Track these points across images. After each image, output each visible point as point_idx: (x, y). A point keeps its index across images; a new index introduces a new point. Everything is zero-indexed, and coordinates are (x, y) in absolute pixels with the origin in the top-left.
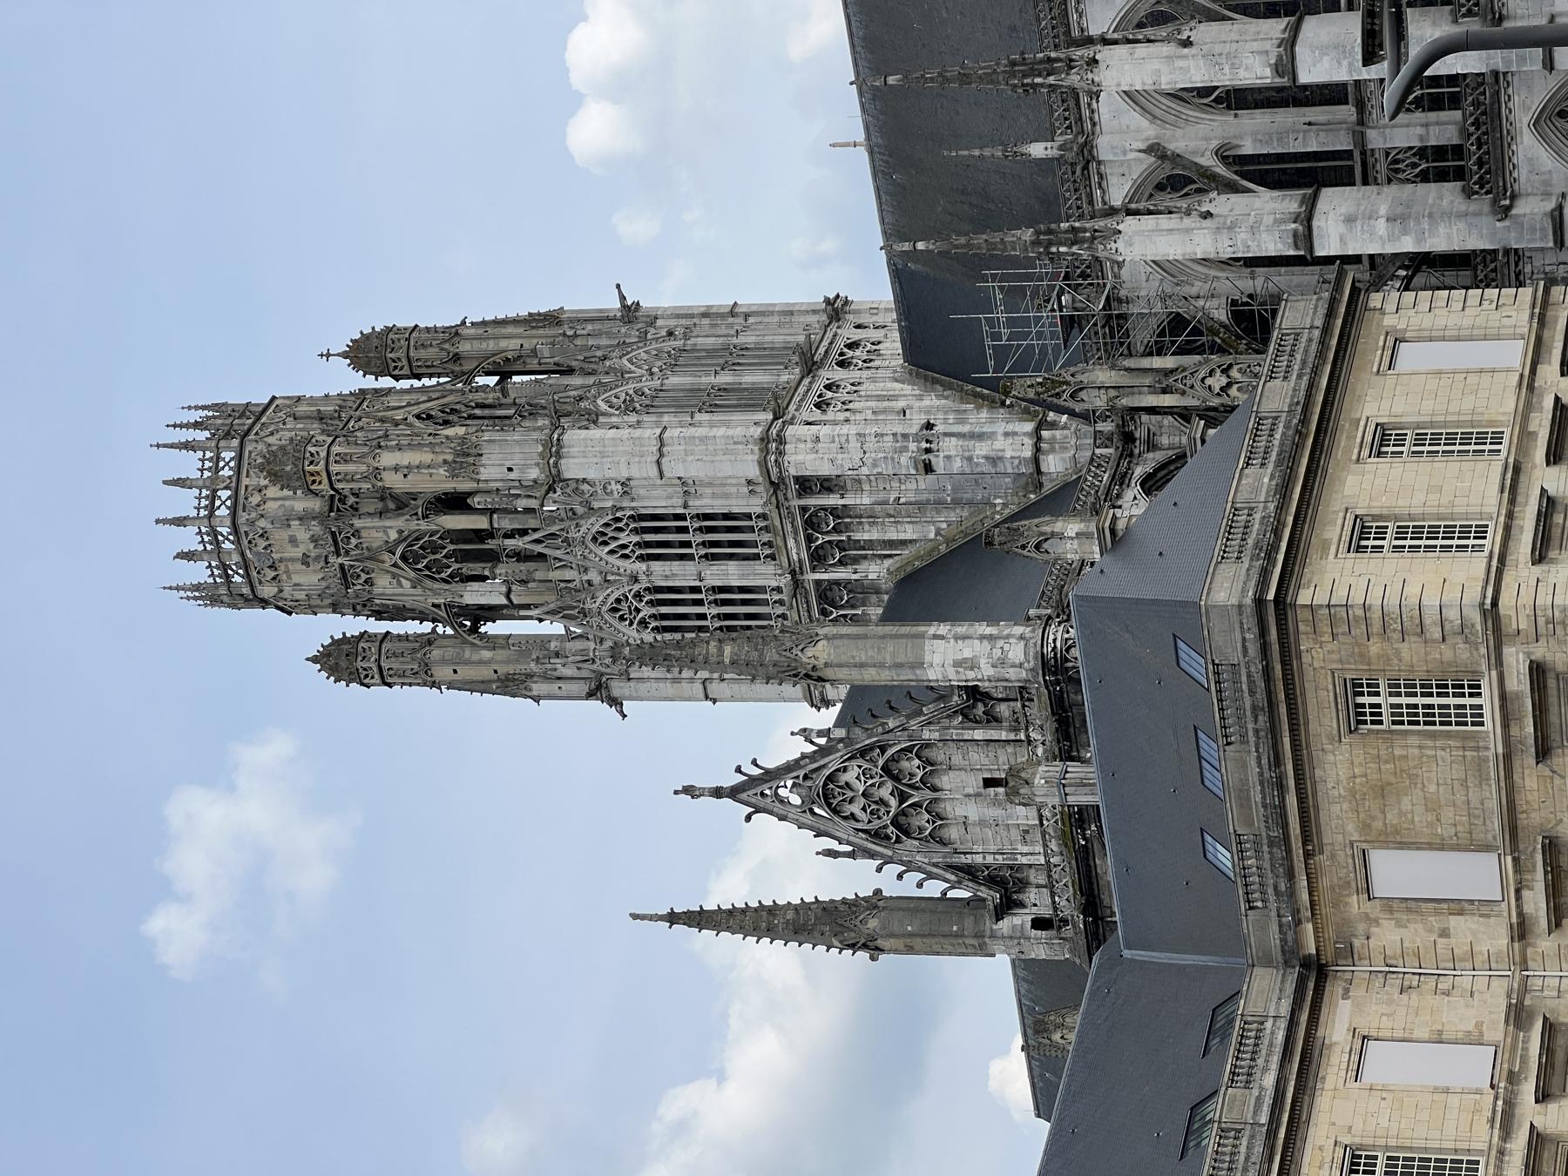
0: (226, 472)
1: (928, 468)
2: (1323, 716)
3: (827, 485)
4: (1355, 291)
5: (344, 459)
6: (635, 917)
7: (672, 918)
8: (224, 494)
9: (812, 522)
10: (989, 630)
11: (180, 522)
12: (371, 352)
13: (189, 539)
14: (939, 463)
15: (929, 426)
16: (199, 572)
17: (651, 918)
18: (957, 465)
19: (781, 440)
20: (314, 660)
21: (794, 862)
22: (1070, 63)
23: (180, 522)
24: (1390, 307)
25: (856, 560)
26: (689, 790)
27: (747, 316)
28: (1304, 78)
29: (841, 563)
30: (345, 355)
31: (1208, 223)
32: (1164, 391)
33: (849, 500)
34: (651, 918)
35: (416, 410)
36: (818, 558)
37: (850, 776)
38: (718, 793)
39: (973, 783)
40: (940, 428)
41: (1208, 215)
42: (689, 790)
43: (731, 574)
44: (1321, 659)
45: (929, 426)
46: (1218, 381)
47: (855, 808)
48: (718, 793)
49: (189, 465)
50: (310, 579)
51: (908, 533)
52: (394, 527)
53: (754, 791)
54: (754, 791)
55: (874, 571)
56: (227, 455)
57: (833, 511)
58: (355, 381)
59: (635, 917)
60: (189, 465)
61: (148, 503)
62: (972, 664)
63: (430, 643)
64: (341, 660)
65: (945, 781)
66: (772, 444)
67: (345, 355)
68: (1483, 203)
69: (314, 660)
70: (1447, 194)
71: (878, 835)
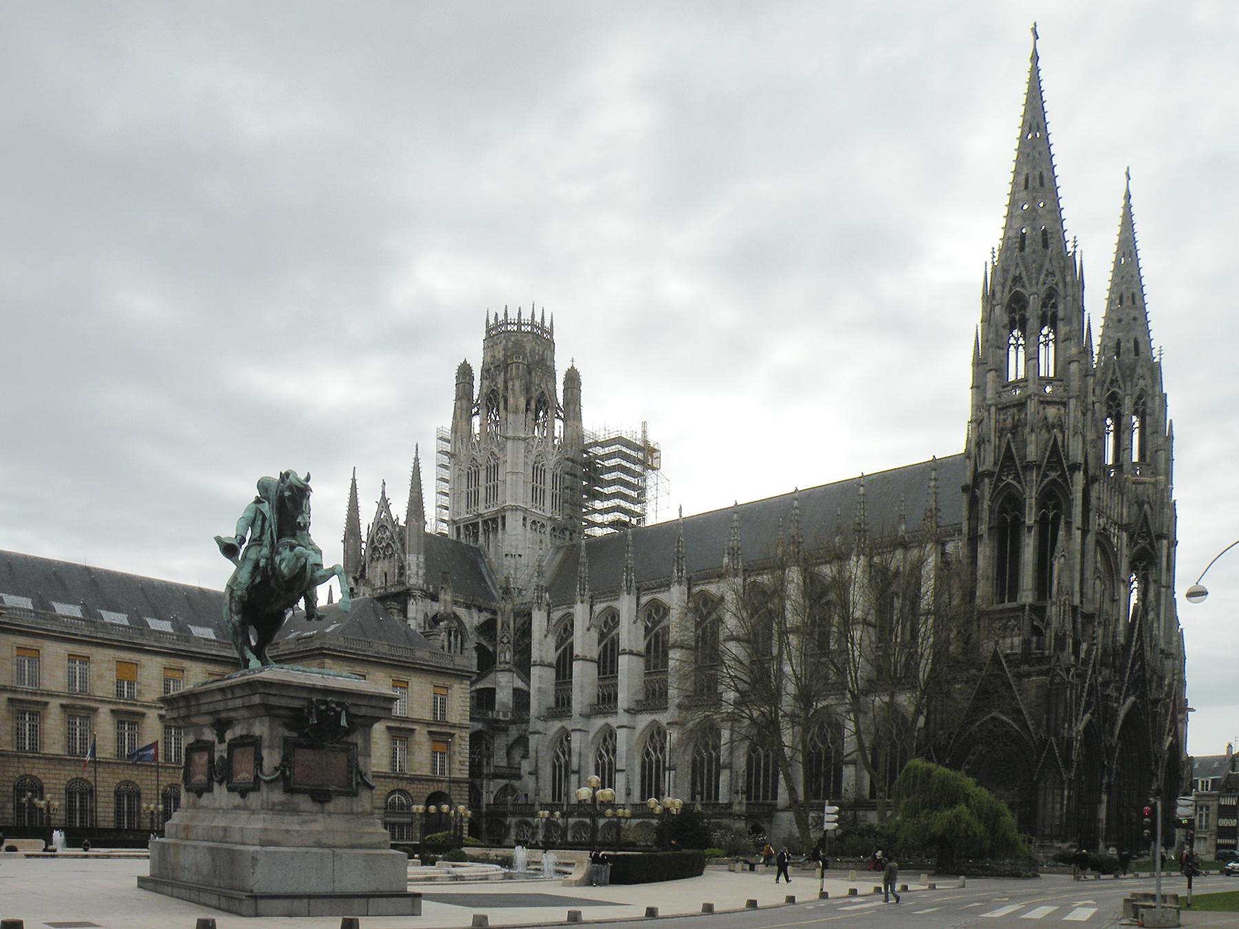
5: (518, 368)
46: (505, 640)
49: (526, 316)
56: (529, 329)
60: (526, 316)
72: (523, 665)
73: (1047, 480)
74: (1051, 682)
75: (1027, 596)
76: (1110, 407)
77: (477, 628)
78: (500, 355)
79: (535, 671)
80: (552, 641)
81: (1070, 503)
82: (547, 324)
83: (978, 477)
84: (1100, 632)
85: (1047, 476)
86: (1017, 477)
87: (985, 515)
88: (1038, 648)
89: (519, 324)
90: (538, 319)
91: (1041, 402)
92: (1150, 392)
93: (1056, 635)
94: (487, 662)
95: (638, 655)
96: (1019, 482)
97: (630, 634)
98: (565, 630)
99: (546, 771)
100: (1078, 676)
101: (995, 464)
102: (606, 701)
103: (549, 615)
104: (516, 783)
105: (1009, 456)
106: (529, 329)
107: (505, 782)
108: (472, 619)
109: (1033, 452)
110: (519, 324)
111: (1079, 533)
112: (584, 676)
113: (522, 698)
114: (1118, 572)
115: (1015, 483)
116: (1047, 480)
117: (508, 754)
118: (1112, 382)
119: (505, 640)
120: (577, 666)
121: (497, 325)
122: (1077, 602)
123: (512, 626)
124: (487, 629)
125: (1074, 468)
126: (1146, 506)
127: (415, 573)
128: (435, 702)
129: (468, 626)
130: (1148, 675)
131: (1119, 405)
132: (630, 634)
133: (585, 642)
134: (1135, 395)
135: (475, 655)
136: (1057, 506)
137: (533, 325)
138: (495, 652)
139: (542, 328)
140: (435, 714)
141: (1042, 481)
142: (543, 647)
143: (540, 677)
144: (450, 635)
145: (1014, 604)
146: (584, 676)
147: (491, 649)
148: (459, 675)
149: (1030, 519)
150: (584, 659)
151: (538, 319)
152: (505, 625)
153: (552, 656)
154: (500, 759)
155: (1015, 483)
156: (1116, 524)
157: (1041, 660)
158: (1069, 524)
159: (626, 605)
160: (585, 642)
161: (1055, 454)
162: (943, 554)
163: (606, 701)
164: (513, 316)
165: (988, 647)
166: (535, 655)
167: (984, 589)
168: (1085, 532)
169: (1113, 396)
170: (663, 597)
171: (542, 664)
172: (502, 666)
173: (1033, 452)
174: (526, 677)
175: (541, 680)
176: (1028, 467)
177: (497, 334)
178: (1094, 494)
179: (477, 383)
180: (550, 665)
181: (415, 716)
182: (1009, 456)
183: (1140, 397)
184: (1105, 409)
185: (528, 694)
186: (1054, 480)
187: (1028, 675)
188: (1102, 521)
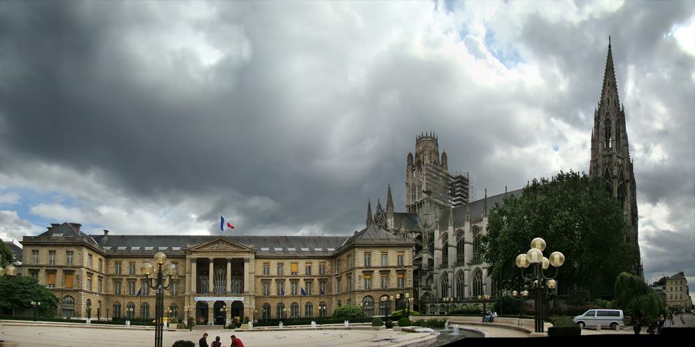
9: (421, 203)
13: (421, 136)
36: (418, 205)
44: (352, 252)
49: (429, 135)
55: (417, 210)
58: (441, 153)
60: (429, 135)
64: (410, 155)
68: (438, 266)
72: (432, 250)
79: (436, 252)
80: (441, 241)
90: (433, 136)
98: (446, 236)
99: (440, 287)
102: (460, 261)
104: (429, 291)
107: (425, 291)
112: (452, 252)
113: (431, 261)
117: (427, 282)
120: (449, 249)
124: (419, 238)
132: (469, 236)
133: (452, 240)
137: (431, 138)
142: (438, 243)
146: (452, 252)
151: (433, 136)
152: (425, 237)
153: (441, 246)
154: (424, 283)
159: (467, 227)
163: (460, 261)
164: (424, 135)
166: (436, 246)
171: (438, 249)
174: (433, 254)
175: (438, 254)
177: (419, 141)
179: (414, 160)
180: (440, 250)
185: (433, 260)
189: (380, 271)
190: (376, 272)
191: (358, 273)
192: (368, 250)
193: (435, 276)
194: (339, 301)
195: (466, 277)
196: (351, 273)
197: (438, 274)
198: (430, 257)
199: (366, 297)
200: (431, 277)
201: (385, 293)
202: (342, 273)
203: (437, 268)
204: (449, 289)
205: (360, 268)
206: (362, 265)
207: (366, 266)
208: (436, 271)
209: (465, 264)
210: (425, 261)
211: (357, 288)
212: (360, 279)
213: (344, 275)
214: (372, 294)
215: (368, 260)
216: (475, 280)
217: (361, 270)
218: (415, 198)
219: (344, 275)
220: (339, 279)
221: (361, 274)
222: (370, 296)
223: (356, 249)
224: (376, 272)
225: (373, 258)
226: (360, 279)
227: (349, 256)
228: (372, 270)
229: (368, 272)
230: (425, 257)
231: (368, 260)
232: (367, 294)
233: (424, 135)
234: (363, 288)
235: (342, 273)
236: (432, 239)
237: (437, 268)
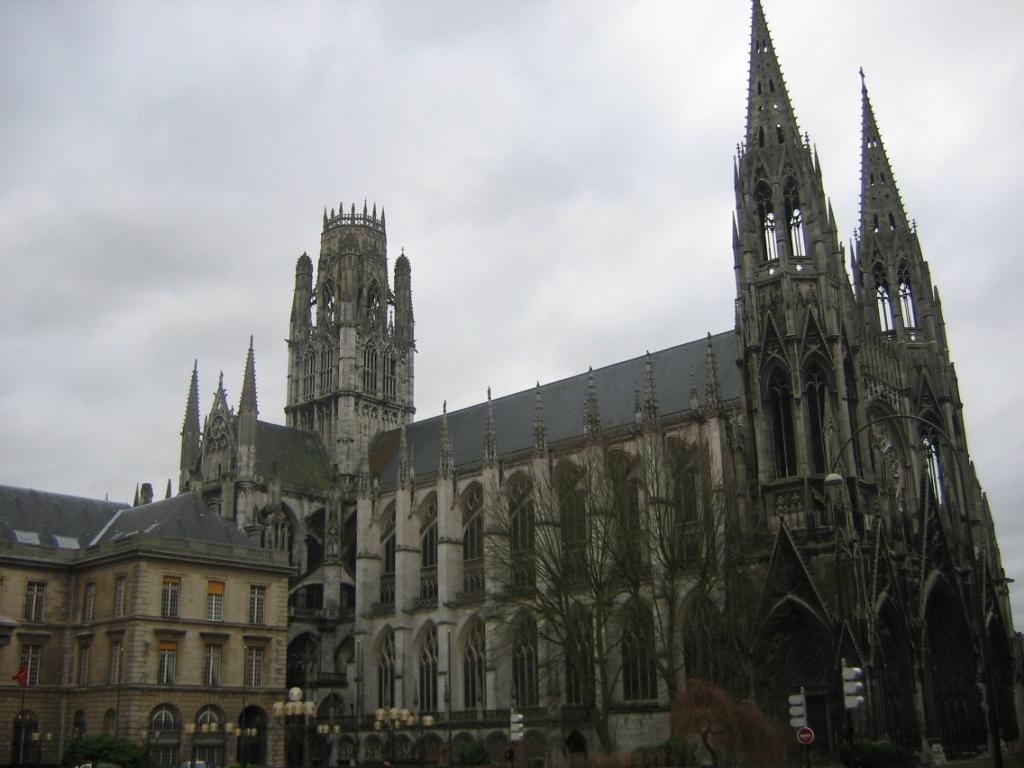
0: (356, 222)
1: (339, 441)
2: (118, 569)
3: (337, 410)
4: (288, 574)
5: (350, 258)
6: (196, 361)
7: (195, 372)
8: (349, 222)
10: (252, 464)
11: (341, 210)
12: (403, 265)
13: (337, 213)
14: (341, 444)
15: (352, 441)
16: (329, 217)
17: (196, 367)
18: (339, 450)
19: (349, 395)
20: (305, 254)
21: (205, 409)
22: (403, 482)
23: (341, 210)
24: (282, 584)
25: (319, 420)
26: (222, 375)
27: (409, 381)
28: (397, 555)
29: (319, 416)
30: (403, 255)
31: (367, 527)
32: (331, 516)
33: (333, 418)
34: (196, 367)
35: (377, 279)
37: (223, 425)
38: (221, 384)
39: (219, 461)
40: (351, 444)
41: (371, 526)
42: (222, 375)
43: (317, 380)
44: (129, 568)
45: (352, 441)
46: (333, 532)
47: (216, 427)
48: (221, 384)
49: (359, 211)
50: (325, 252)
51: (325, 435)
52: (335, 275)
53: (221, 395)
54: (221, 395)
55: (316, 426)
56: (362, 222)
57: (331, 413)
59: (196, 361)
60: (359, 211)
61: (353, 199)
62: (241, 460)
63: (307, 290)
64: (304, 263)
65: (221, 453)
66: (347, 394)
67: (403, 255)
69: (305, 254)
70: (376, 596)
71: (209, 433)
73: (808, 353)
74: (838, 558)
75: (805, 470)
76: (877, 277)
77: (307, 519)
78: (335, 247)
79: (360, 564)
81: (833, 373)
82: (379, 217)
83: (748, 352)
84: (885, 505)
85: (809, 349)
86: (781, 352)
87: (758, 389)
88: (823, 523)
89: (353, 218)
90: (370, 213)
91: (759, 288)
92: (910, 261)
93: (835, 509)
94: (316, 558)
95: (456, 543)
96: (784, 356)
97: (449, 523)
98: (389, 518)
100: (865, 551)
101: (760, 340)
103: (412, 494)
105: (771, 331)
106: (362, 222)
108: (302, 509)
109: (792, 327)
110: (353, 218)
111: (845, 405)
112: (406, 566)
114: (907, 439)
115: (779, 357)
116: (808, 353)
118: (875, 253)
119: (333, 532)
120: (399, 557)
121: (334, 219)
122: (853, 473)
123: (339, 516)
124: (316, 520)
125: (832, 340)
126: (924, 371)
127: (247, 470)
128: (252, 603)
129: (298, 517)
130: (950, 544)
131: (884, 275)
133: (407, 532)
134: (898, 264)
135: (305, 548)
136: (822, 378)
137: (365, 218)
138: (323, 544)
139: (374, 220)
140: (252, 617)
141: (804, 354)
142: (368, 539)
143: (365, 570)
144: (277, 528)
145: (794, 478)
146: (406, 566)
147: (320, 541)
148: (276, 573)
149: (798, 392)
150: (406, 550)
151: (370, 213)
155: (779, 357)
156: (895, 389)
157: (827, 536)
158: (834, 395)
160: (407, 532)
161: (813, 329)
162: (728, 428)
164: (347, 211)
165: (774, 521)
166: (360, 547)
167: (764, 464)
168: (853, 402)
169: (878, 267)
170: (480, 479)
171: (367, 557)
172: (330, 561)
173: (792, 327)
175: (366, 573)
176: (789, 341)
177: (333, 226)
178: (857, 365)
179: (315, 274)
181: (231, 619)
182: (771, 331)
183: (902, 267)
184: (872, 279)
186: (815, 353)
187: (816, 552)
188: (880, 388)
189: (203, 635)
190: (192, 635)
191: (143, 634)
192: (174, 571)
193: (358, 639)
194: (80, 713)
195: (443, 647)
196: (122, 632)
197: (367, 632)
198: (346, 579)
199: (159, 707)
200: (348, 642)
201: (214, 700)
202: (95, 625)
203: (364, 616)
204: (398, 684)
205: (148, 620)
206: (154, 611)
207: (164, 614)
208: (361, 624)
209: (440, 604)
210: (331, 593)
211: (136, 678)
212: (146, 653)
213: (101, 632)
214: (175, 699)
215: (171, 599)
216: (470, 653)
217: (151, 627)
218: (312, 389)
219: (101, 632)
220: (85, 642)
221: (149, 638)
222: (169, 707)
223: (143, 565)
224: (192, 635)
225: (185, 595)
226: (146, 653)
227: (120, 578)
228: (178, 628)
229: (170, 637)
230: (331, 579)
231: (171, 599)
232: (162, 699)
233: (347, 211)
234: (152, 681)
235: (95, 625)
236: (352, 522)
237: (364, 616)
